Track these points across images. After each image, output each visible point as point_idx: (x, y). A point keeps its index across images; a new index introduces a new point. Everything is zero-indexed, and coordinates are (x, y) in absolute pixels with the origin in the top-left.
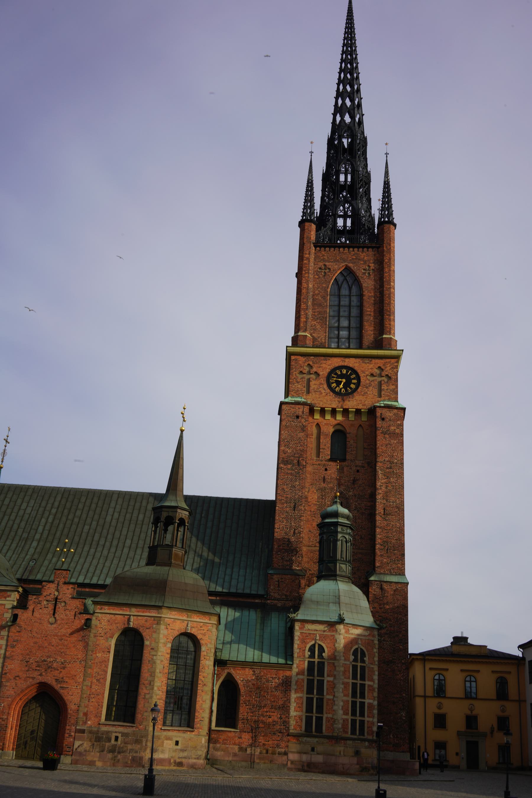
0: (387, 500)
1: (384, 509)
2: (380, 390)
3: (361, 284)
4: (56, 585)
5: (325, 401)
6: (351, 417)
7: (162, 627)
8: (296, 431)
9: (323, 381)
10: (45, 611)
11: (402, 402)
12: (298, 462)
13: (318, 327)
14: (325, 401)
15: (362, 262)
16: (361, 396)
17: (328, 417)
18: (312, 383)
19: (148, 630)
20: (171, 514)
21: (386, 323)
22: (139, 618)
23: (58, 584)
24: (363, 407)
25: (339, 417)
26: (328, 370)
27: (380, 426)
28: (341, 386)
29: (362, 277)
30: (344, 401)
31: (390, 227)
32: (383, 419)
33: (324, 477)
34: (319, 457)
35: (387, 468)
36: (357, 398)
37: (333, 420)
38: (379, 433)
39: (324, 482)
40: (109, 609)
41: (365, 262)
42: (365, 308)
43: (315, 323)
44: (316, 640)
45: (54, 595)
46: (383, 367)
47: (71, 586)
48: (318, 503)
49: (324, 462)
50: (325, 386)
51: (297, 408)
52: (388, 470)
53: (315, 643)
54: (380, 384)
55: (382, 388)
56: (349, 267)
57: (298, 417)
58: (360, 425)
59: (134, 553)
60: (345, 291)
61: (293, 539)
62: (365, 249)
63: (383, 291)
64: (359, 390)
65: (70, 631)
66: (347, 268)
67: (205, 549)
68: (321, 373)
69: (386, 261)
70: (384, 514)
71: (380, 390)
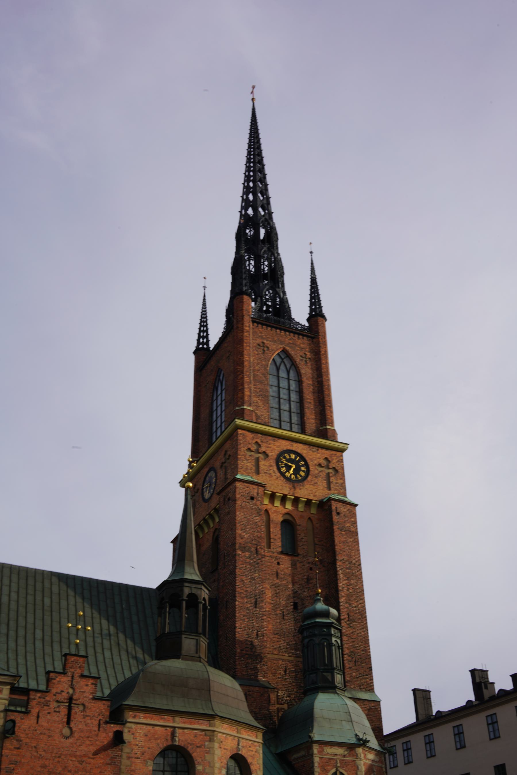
0: (350, 604)
1: (348, 614)
2: (329, 483)
3: (299, 370)
4: (70, 679)
6: (301, 507)
7: (216, 745)
8: (252, 513)
9: (272, 462)
10: (56, 717)
11: (351, 497)
12: (257, 550)
13: (261, 404)
15: (298, 349)
16: (311, 486)
17: (277, 503)
18: (262, 463)
19: (198, 750)
20: (194, 591)
21: (328, 413)
22: (186, 731)
23: (73, 677)
24: (316, 499)
25: (289, 506)
26: (277, 452)
27: (336, 521)
28: (291, 471)
29: (300, 364)
30: (294, 488)
32: (338, 514)
33: (277, 572)
34: (270, 548)
35: (347, 568)
36: (307, 486)
37: (281, 508)
38: (335, 527)
39: (277, 577)
40: (145, 718)
41: (302, 349)
42: (304, 395)
43: (257, 399)
44: (336, 766)
45: (68, 693)
46: (330, 459)
47: (91, 681)
48: (273, 602)
49: (275, 555)
50: (275, 469)
51: (251, 488)
53: (337, 770)
54: (328, 476)
55: (331, 480)
56: (287, 351)
57: (252, 498)
58: (309, 518)
59: (50, 648)
60: (283, 374)
61: (256, 642)
62: (301, 336)
63: (322, 381)
64: (309, 478)
65: (93, 749)
66: (284, 351)
67: (138, 649)
68: (270, 454)
69: (323, 352)
70: (348, 620)
71: (329, 483)
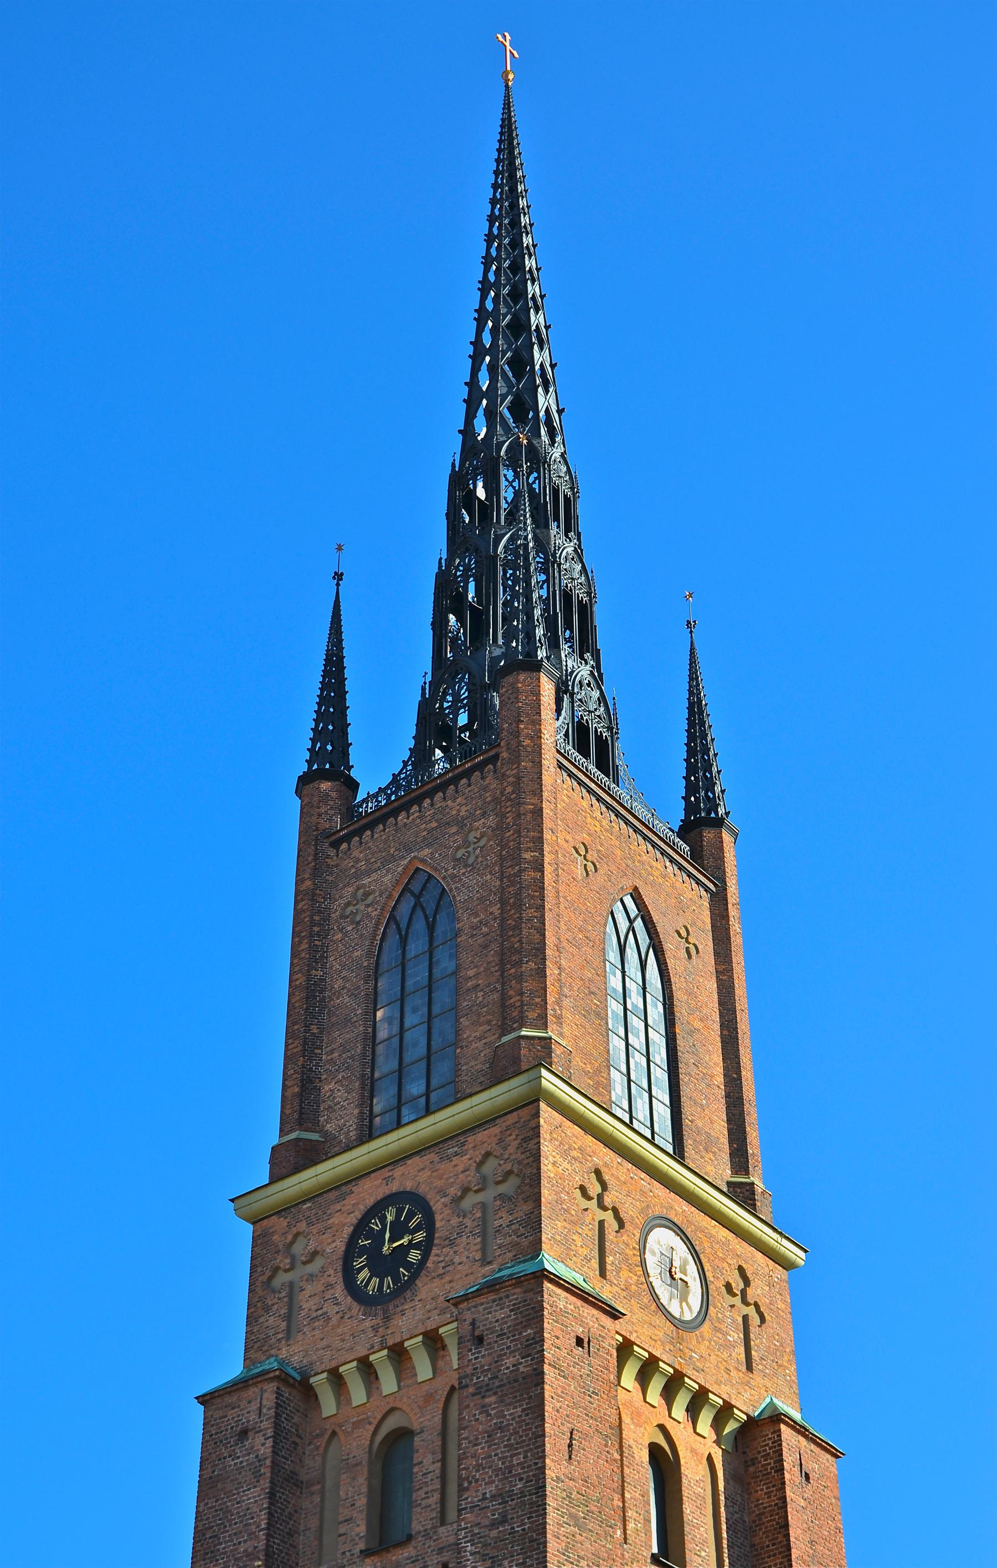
5: (338, 1344)
14: (338, 1344)
30: (387, 1318)
31: (513, 685)
35: (494, 1525)
50: (339, 1291)
52: (494, 1533)
